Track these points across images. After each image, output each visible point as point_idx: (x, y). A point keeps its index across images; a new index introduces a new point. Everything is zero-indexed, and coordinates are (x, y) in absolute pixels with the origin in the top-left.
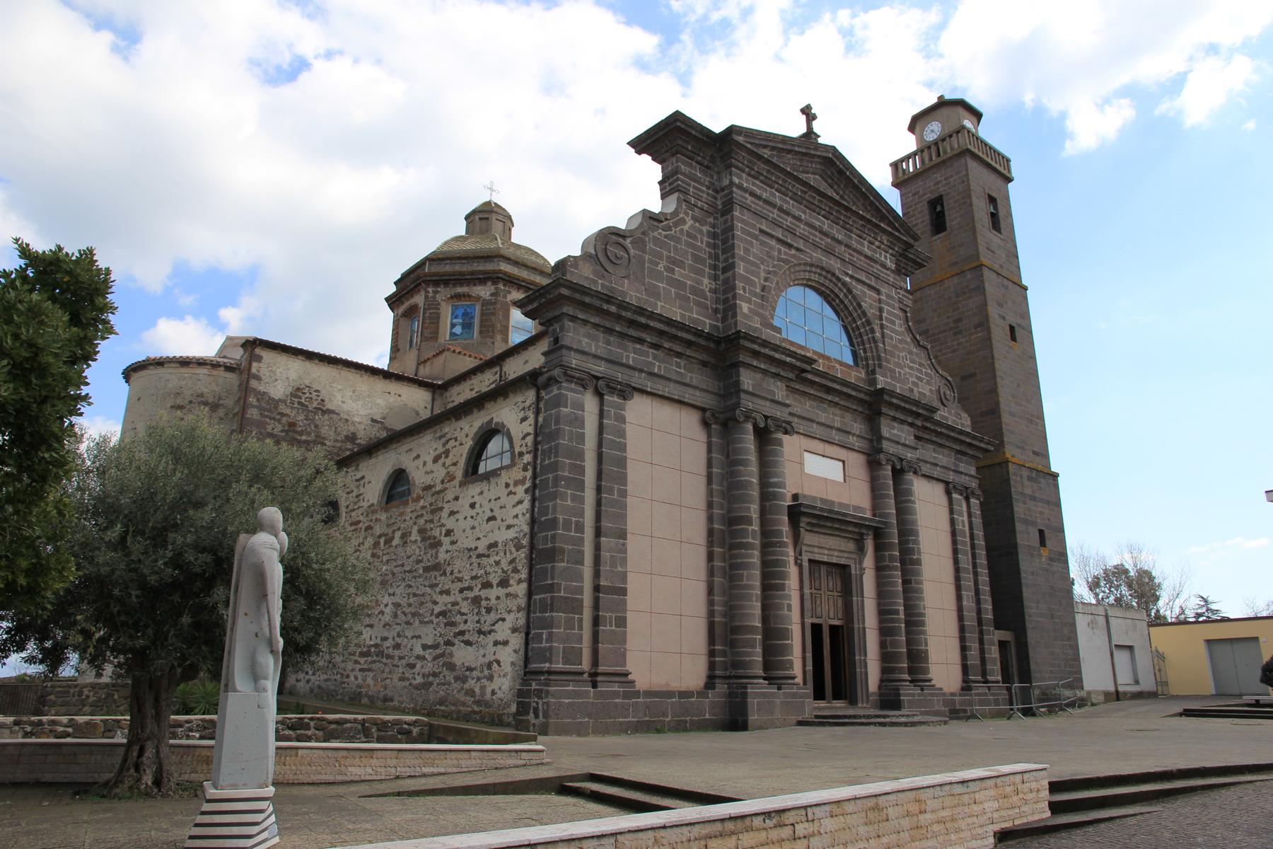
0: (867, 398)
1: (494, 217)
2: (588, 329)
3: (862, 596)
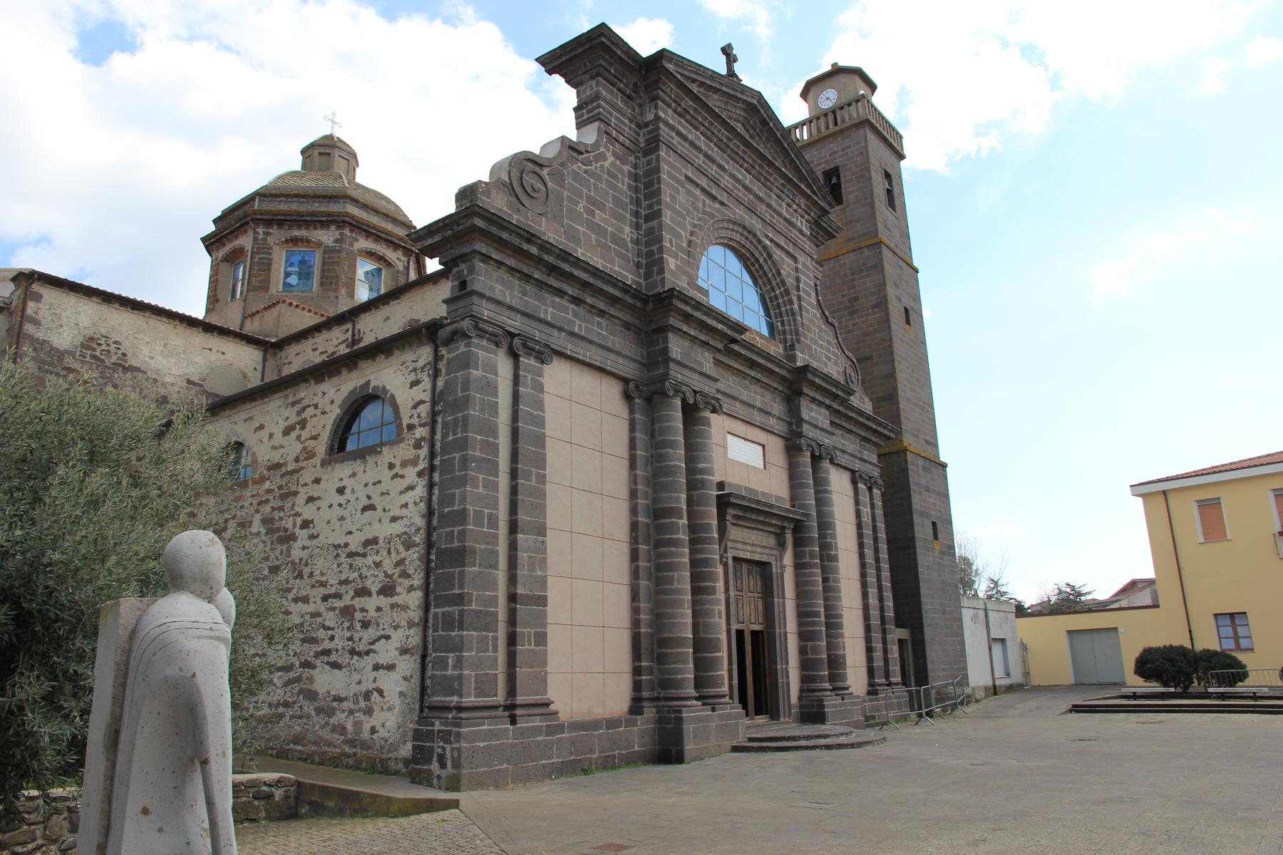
0: (788, 376)
1: (336, 153)
2: (502, 274)
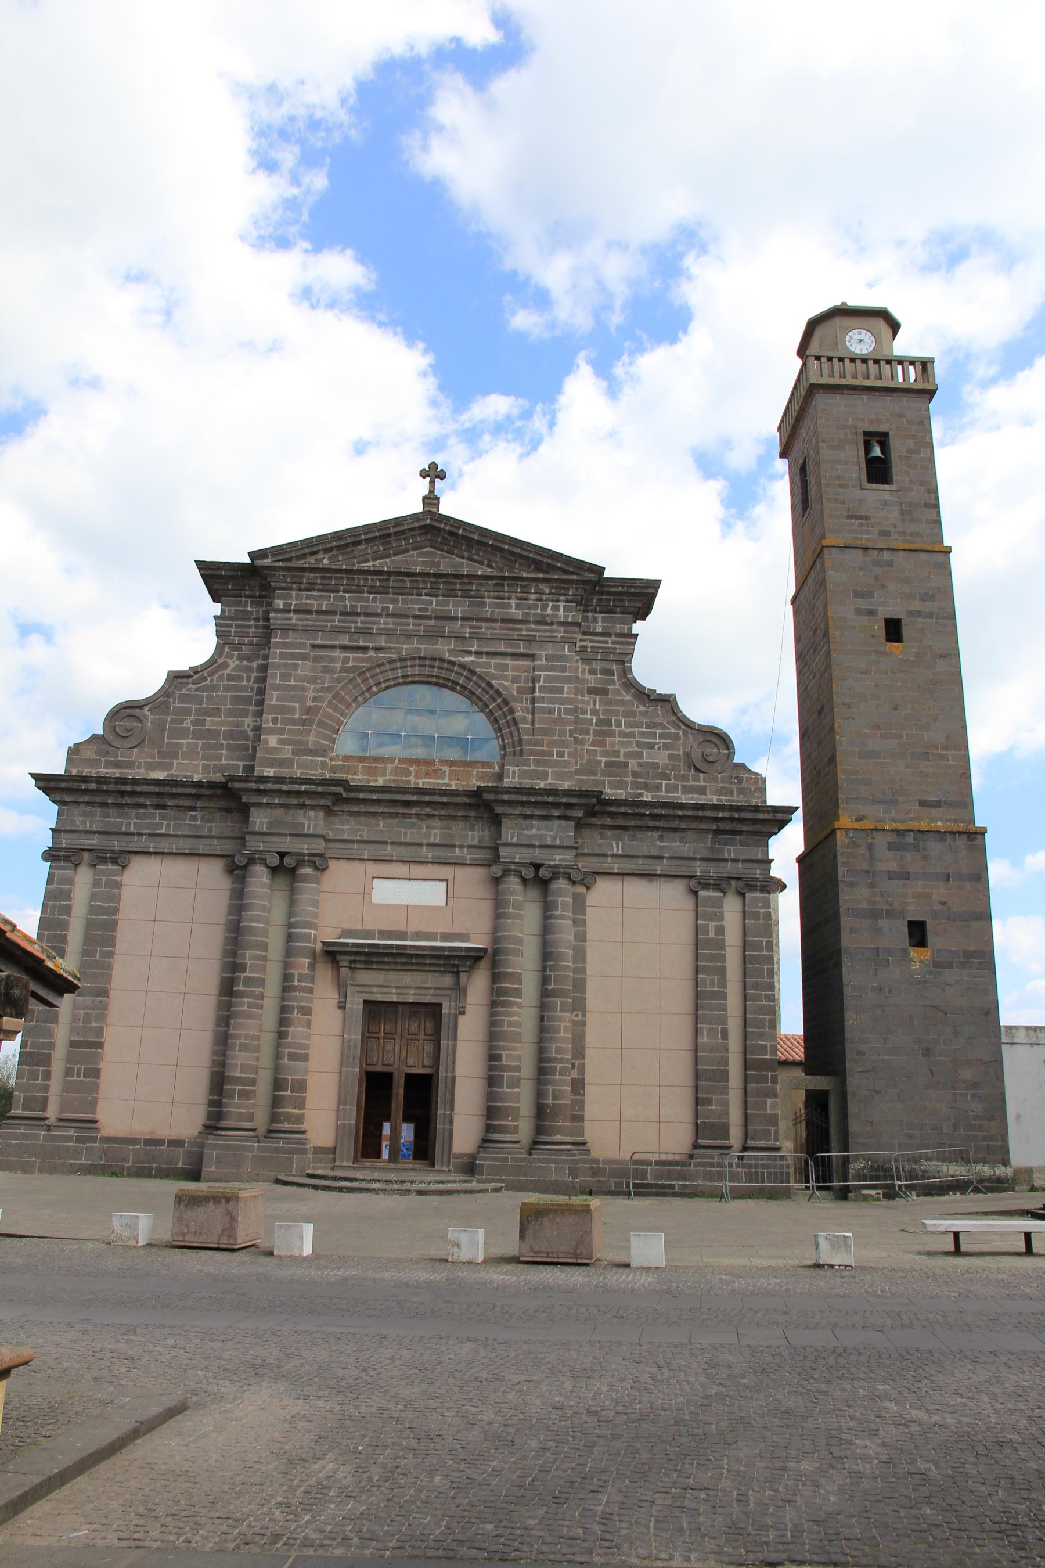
2: (83, 807)
3: (455, 1039)
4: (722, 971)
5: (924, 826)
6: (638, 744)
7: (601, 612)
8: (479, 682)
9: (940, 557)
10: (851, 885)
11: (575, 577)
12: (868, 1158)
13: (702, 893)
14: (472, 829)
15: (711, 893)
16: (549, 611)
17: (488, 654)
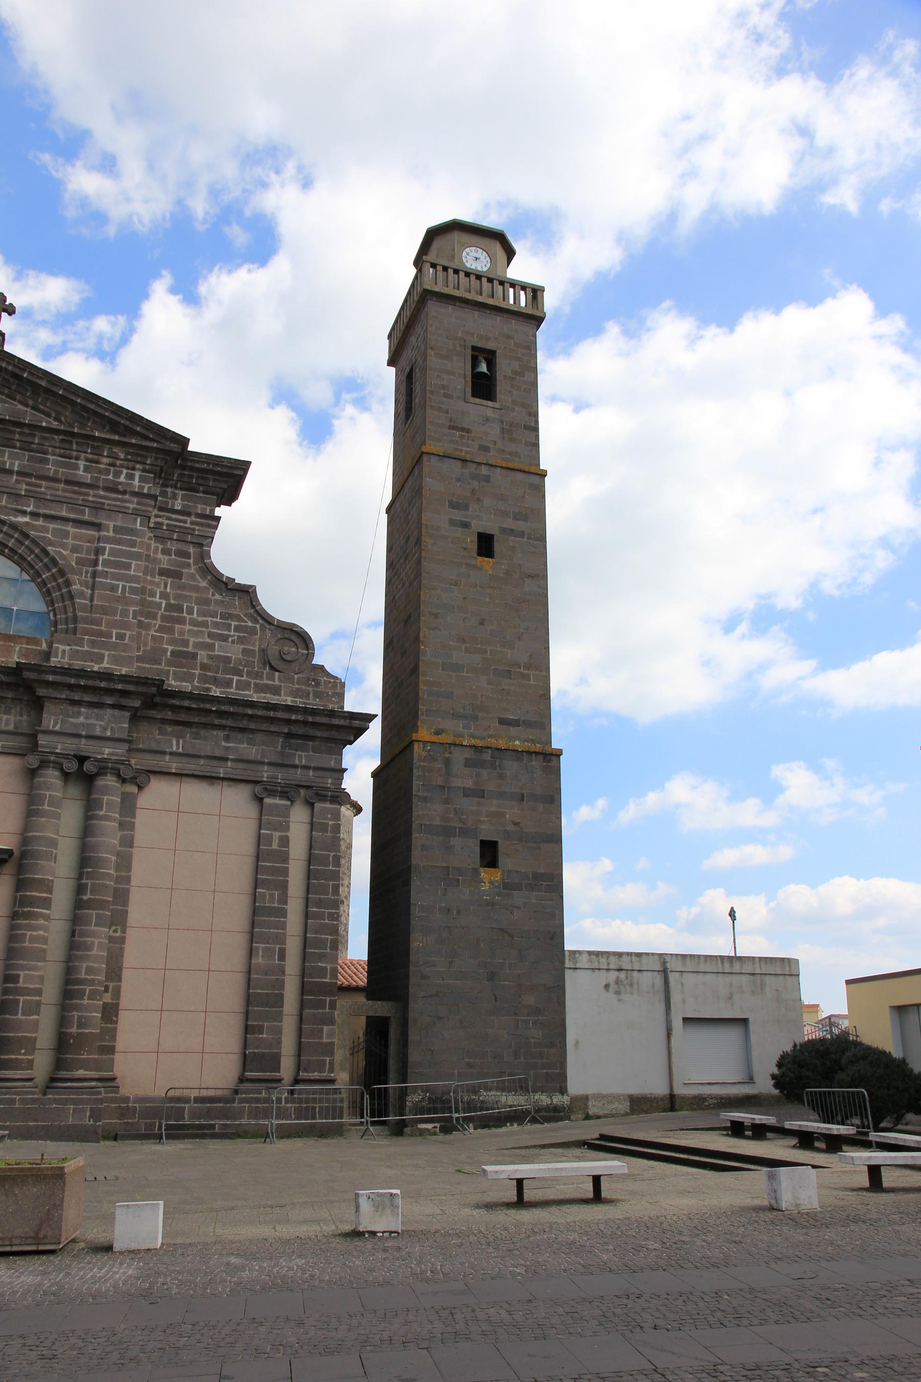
4: (283, 887)
5: (502, 744)
6: (210, 635)
7: (181, 489)
8: (32, 546)
9: (535, 479)
10: (425, 799)
11: (155, 445)
12: (426, 1089)
13: (268, 801)
14: (8, 712)
15: (278, 801)
16: (122, 479)
17: (46, 517)
